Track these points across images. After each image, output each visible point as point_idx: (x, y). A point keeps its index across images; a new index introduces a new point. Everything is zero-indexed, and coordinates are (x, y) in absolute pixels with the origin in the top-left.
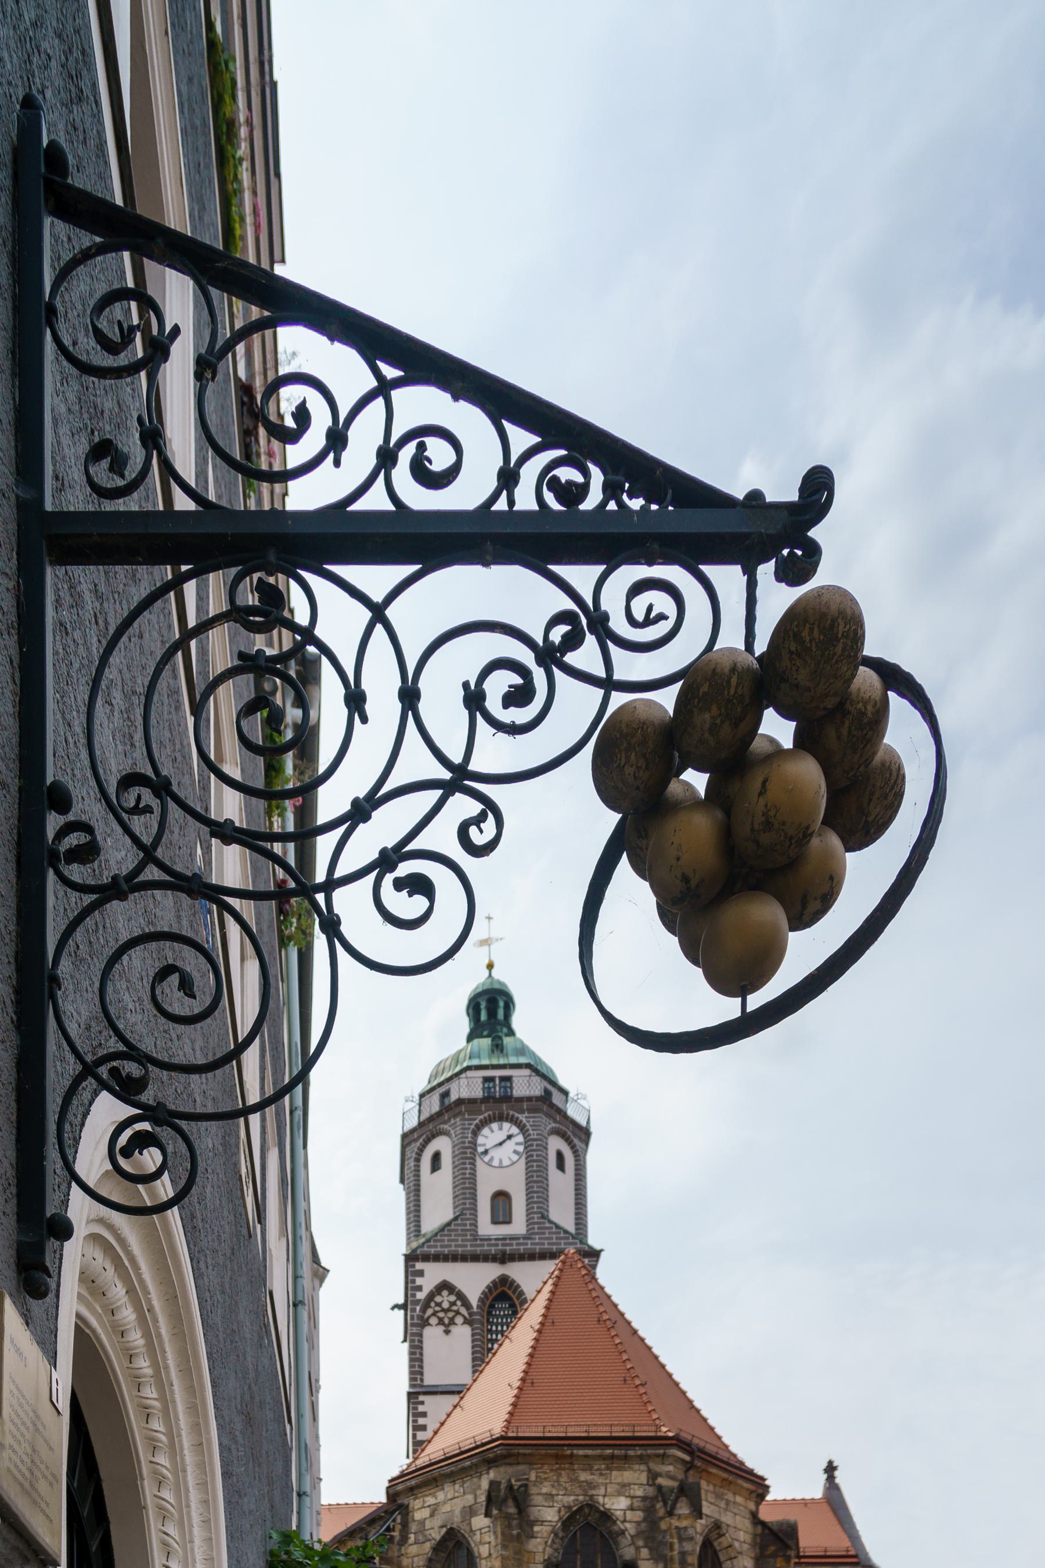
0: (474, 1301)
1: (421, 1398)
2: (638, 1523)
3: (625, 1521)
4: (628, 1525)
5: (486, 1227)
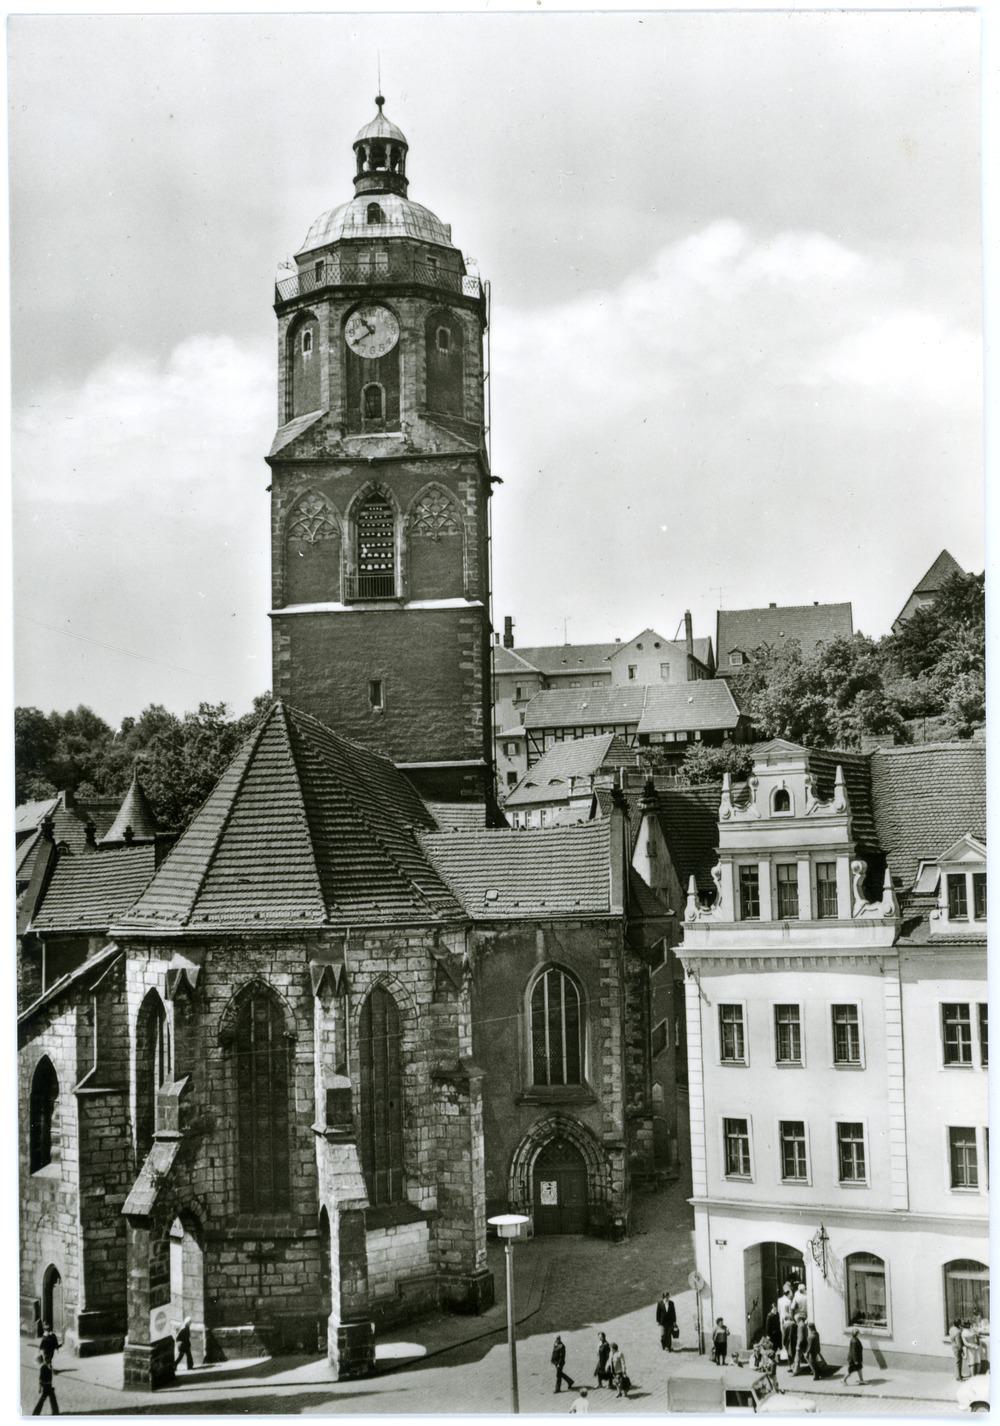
2: (298, 997)
3: (287, 996)
4: (290, 999)
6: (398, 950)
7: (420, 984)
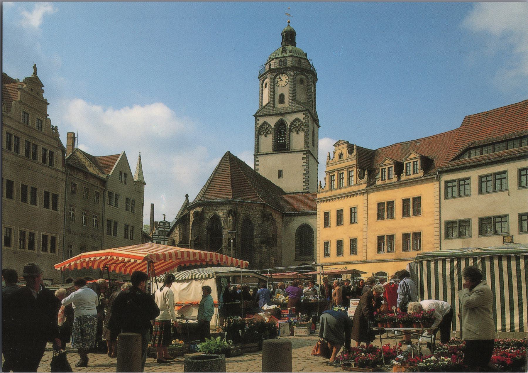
0: (273, 127)
1: (257, 156)
2: (225, 218)
5: (278, 106)
6: (253, 209)
7: (258, 219)
